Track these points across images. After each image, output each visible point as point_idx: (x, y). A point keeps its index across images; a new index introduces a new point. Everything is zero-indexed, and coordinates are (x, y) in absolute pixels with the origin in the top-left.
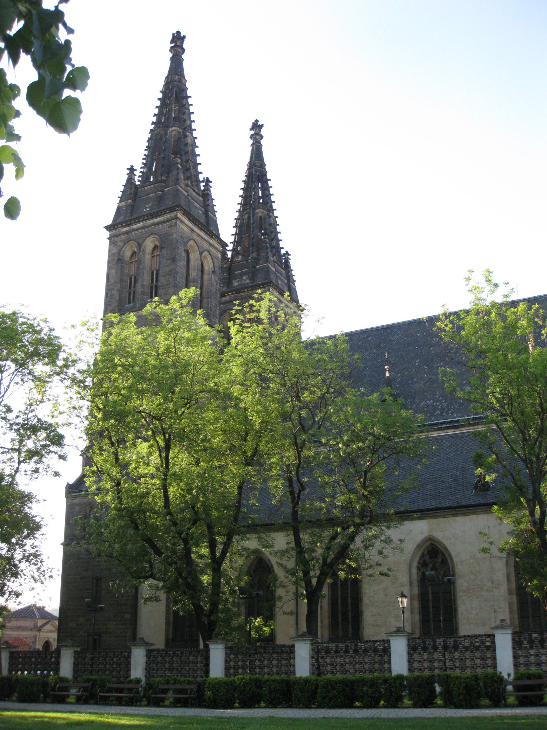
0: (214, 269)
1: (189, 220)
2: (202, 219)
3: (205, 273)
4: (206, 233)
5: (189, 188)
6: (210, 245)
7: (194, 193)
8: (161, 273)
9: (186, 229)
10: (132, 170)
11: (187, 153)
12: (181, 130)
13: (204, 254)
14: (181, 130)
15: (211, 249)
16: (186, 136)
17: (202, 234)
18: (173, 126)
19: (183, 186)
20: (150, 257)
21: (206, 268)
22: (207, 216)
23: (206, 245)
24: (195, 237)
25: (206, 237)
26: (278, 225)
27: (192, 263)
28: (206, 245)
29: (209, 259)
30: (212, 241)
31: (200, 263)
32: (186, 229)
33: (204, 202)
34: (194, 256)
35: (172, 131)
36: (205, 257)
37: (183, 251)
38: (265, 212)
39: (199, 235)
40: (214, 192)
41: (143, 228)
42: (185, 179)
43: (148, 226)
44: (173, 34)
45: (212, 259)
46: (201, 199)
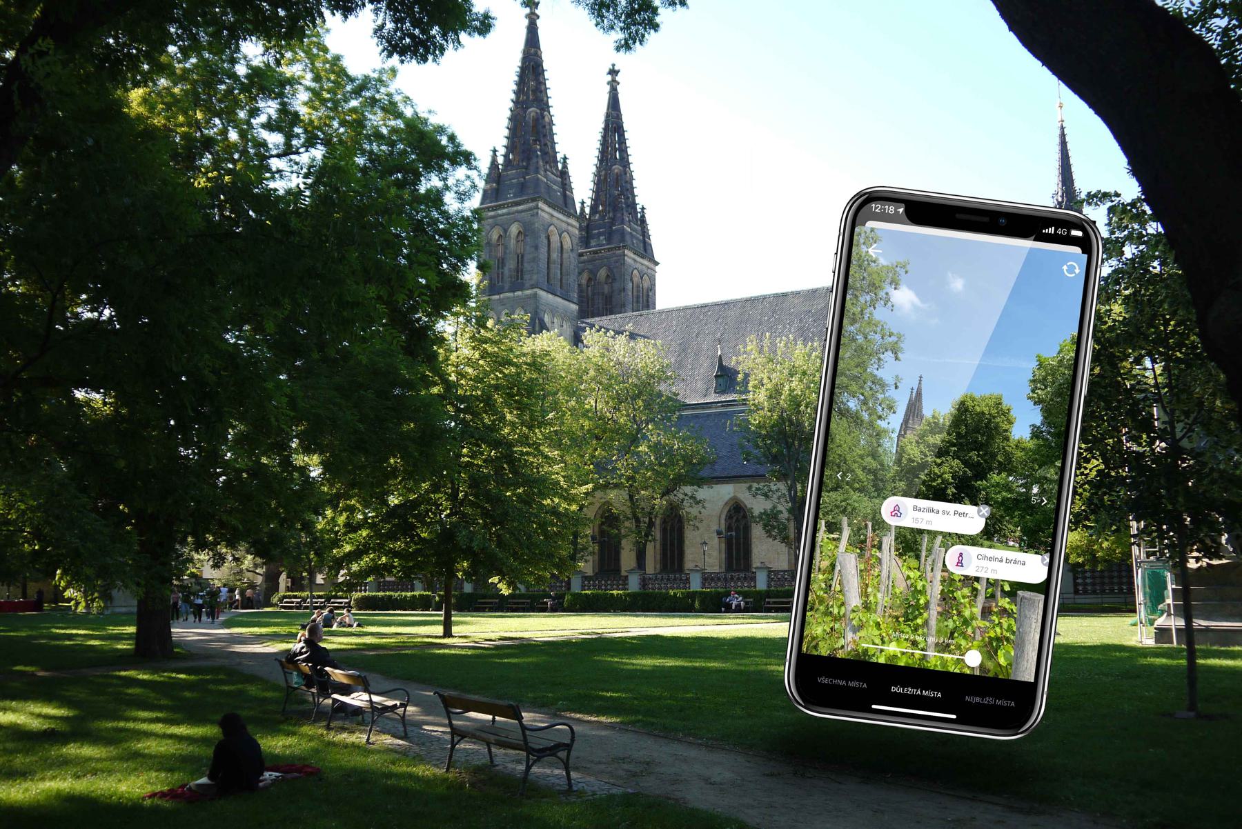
1: (549, 206)
2: (561, 202)
6: (568, 224)
7: (553, 176)
8: (525, 258)
10: (495, 151)
12: (538, 111)
16: (543, 117)
17: (561, 216)
22: (565, 196)
23: (564, 225)
24: (555, 221)
27: (553, 245)
28: (564, 225)
29: (568, 238)
31: (559, 244)
33: (562, 182)
34: (555, 238)
35: (530, 113)
39: (558, 219)
40: (572, 170)
41: (508, 214)
43: (513, 213)
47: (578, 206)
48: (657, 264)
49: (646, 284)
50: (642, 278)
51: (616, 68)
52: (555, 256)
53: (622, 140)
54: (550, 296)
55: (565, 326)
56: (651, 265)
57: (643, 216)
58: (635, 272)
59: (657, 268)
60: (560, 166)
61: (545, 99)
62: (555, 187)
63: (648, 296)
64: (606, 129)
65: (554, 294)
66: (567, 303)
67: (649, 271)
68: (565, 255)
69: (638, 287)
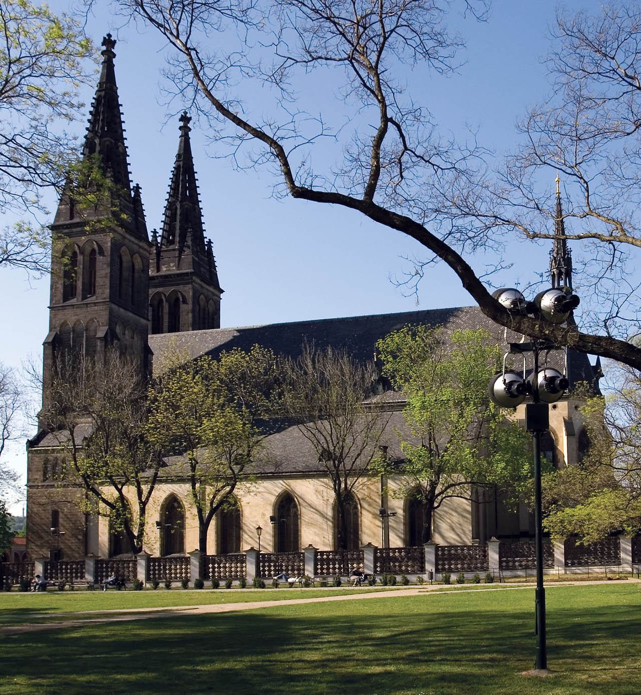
0: (143, 267)
3: (136, 271)
4: (136, 238)
6: (140, 247)
14: (113, 141)
15: (141, 250)
17: (133, 239)
18: (106, 137)
20: (88, 259)
21: (136, 267)
24: (126, 242)
25: (136, 241)
26: (203, 216)
27: (124, 264)
28: (136, 247)
29: (139, 260)
31: (131, 264)
34: (126, 258)
35: (105, 141)
38: (191, 204)
44: (104, 38)
45: (142, 259)
46: (132, 206)
47: (150, 235)
48: (222, 291)
49: (211, 308)
50: (207, 302)
51: (188, 115)
52: (126, 274)
53: (193, 180)
54: (122, 310)
55: (136, 338)
56: (217, 292)
57: (210, 248)
58: (202, 296)
59: (222, 296)
60: (133, 194)
61: (120, 131)
63: (213, 319)
64: (177, 168)
65: (126, 309)
66: (137, 317)
67: (215, 297)
68: (136, 275)
69: (204, 310)
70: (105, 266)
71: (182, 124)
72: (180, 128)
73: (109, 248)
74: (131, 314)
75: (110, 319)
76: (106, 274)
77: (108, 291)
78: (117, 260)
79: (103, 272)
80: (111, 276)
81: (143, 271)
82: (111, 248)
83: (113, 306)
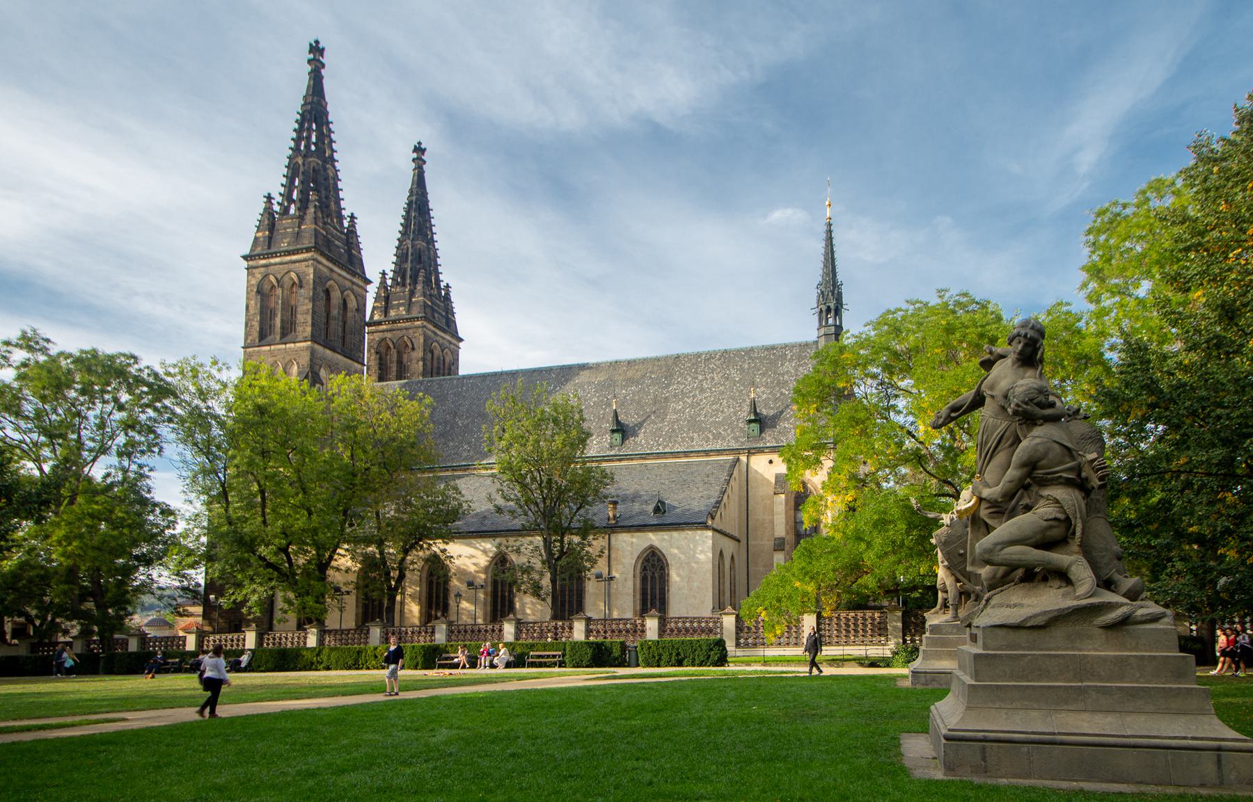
1: (328, 260)
5: (329, 226)
6: (353, 283)
9: (325, 270)
11: (327, 189)
13: (346, 293)
15: (355, 287)
17: (344, 273)
19: (321, 225)
22: (350, 256)
24: (335, 276)
25: (349, 277)
28: (348, 284)
30: (355, 280)
31: (341, 302)
32: (325, 270)
33: (347, 240)
34: (336, 295)
36: (348, 295)
37: (321, 291)
39: (340, 275)
40: (360, 230)
42: (323, 218)
45: (356, 297)
51: (423, 146)
52: (335, 312)
54: (328, 352)
60: (346, 224)
62: (337, 242)
68: (349, 314)
70: (307, 301)
71: (415, 155)
72: (414, 160)
73: (312, 281)
74: (340, 357)
75: (311, 360)
76: (308, 310)
77: (309, 329)
78: (322, 294)
79: (305, 308)
80: (314, 312)
81: (358, 310)
82: (314, 281)
83: (316, 346)
